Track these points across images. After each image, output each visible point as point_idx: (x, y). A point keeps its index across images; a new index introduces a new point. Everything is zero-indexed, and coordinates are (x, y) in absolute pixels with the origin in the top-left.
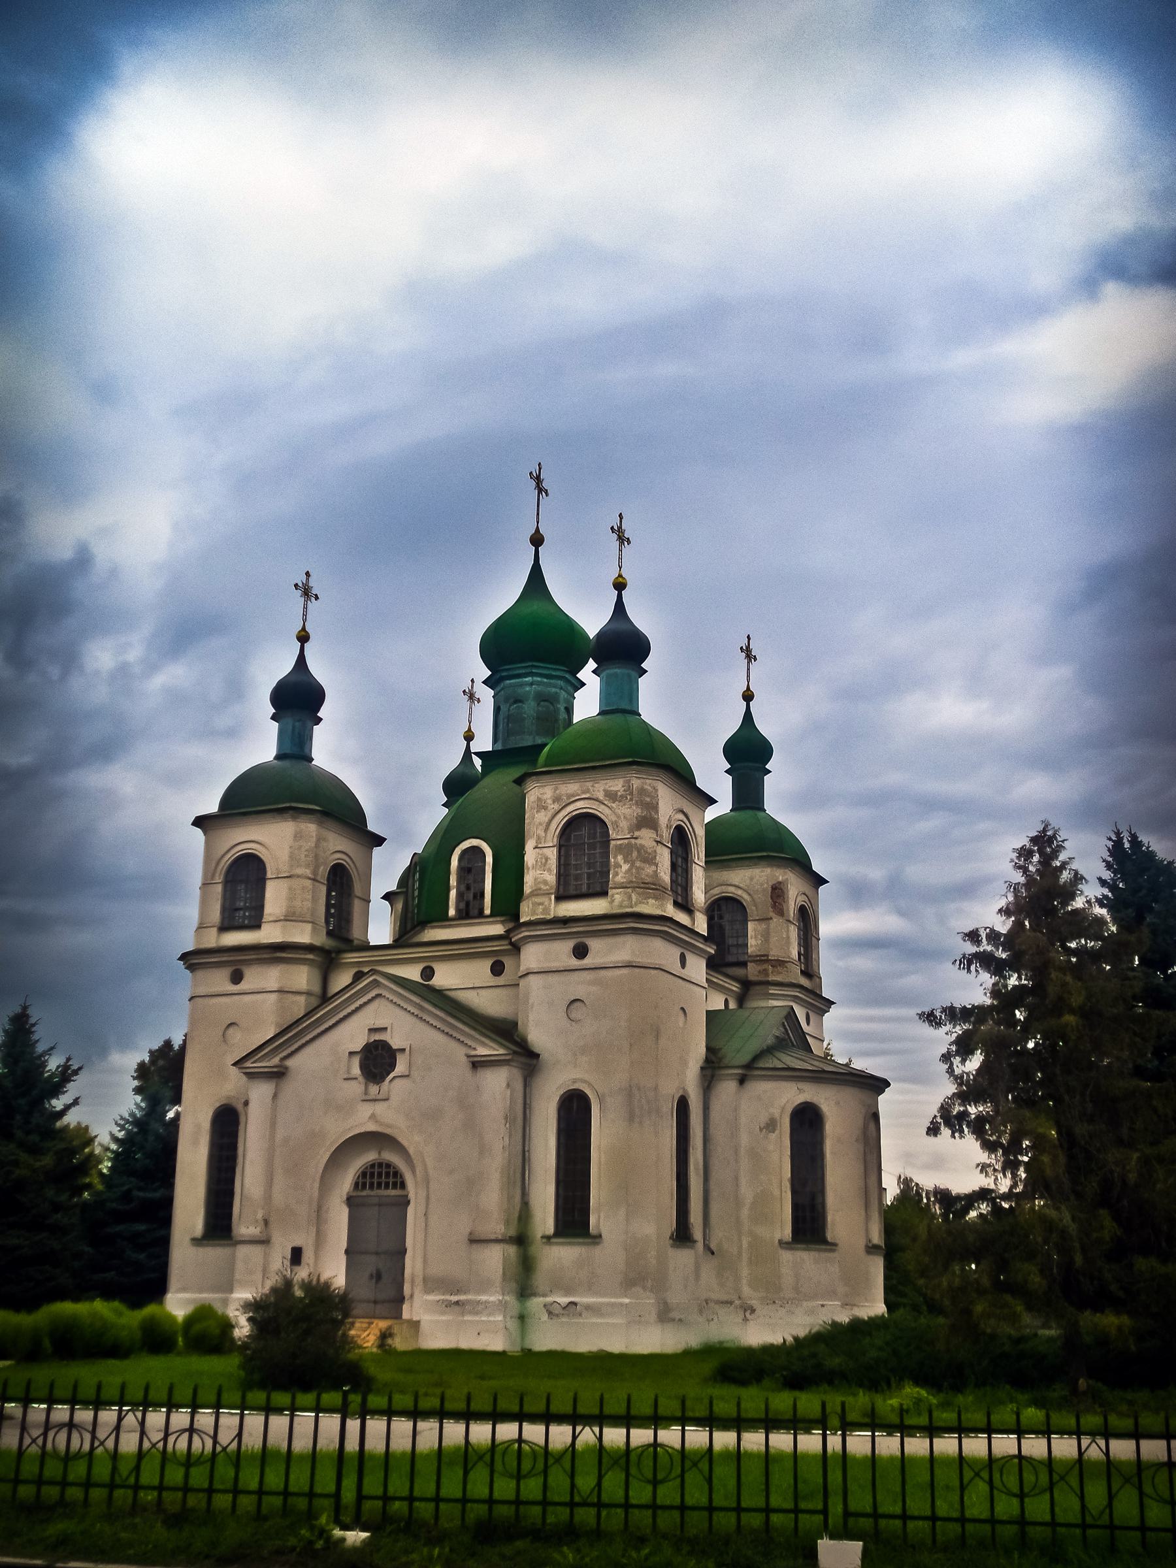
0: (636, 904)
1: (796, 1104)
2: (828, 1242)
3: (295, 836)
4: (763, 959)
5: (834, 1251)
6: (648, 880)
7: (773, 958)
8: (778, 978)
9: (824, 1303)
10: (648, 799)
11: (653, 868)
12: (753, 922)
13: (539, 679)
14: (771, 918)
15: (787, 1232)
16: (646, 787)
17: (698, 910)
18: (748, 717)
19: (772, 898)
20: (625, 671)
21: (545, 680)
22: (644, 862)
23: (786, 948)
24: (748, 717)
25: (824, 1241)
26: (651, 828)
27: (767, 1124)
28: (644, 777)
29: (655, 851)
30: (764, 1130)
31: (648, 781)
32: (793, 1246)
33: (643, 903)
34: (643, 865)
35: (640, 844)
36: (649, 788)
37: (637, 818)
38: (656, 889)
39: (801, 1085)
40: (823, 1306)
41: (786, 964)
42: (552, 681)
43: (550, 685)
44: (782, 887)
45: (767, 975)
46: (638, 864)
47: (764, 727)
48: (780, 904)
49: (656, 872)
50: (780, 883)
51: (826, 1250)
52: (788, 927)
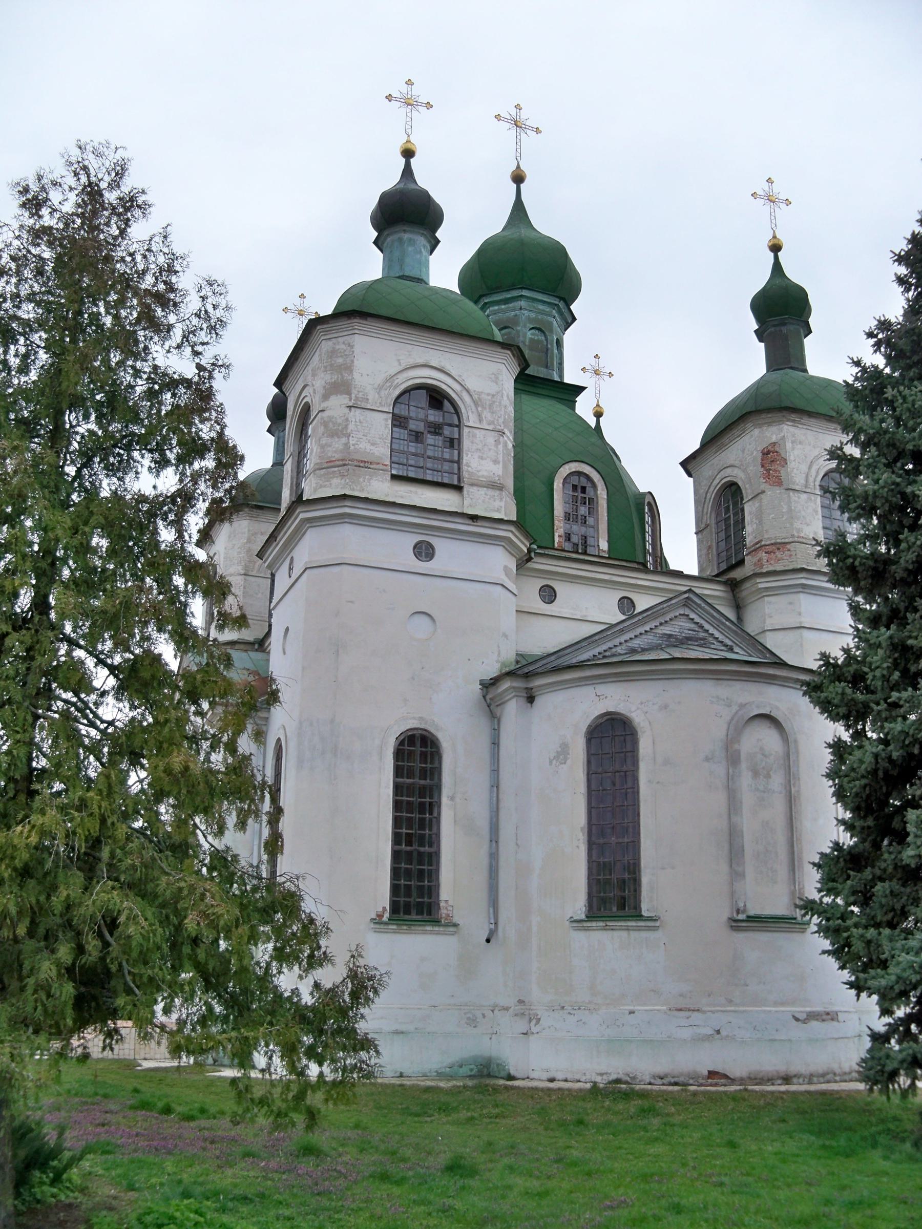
0: (315, 490)
1: (593, 718)
2: (642, 916)
3: (230, 537)
4: (758, 547)
5: (655, 928)
6: (337, 456)
7: (768, 543)
8: (779, 567)
9: (631, 1008)
10: (340, 360)
11: (344, 440)
12: (750, 503)
13: (496, 308)
14: (763, 492)
15: (578, 905)
16: (337, 347)
17: (472, 485)
18: (777, 268)
19: (763, 466)
20: (396, 237)
21: (503, 307)
22: (332, 436)
23: (788, 525)
24: (777, 268)
25: (639, 916)
26: (342, 393)
27: (557, 752)
28: (336, 335)
29: (347, 420)
30: (554, 762)
31: (340, 340)
32: (589, 924)
33: (325, 486)
34: (330, 440)
35: (329, 417)
36: (343, 347)
37: (324, 387)
38: (344, 465)
39: (602, 689)
40: (632, 1012)
41: (788, 546)
42: (511, 305)
43: (508, 310)
44: (777, 449)
45: (762, 566)
46: (324, 441)
47: (793, 274)
48: (775, 471)
49: (347, 445)
50: (774, 444)
51: (639, 929)
52: (789, 496)
